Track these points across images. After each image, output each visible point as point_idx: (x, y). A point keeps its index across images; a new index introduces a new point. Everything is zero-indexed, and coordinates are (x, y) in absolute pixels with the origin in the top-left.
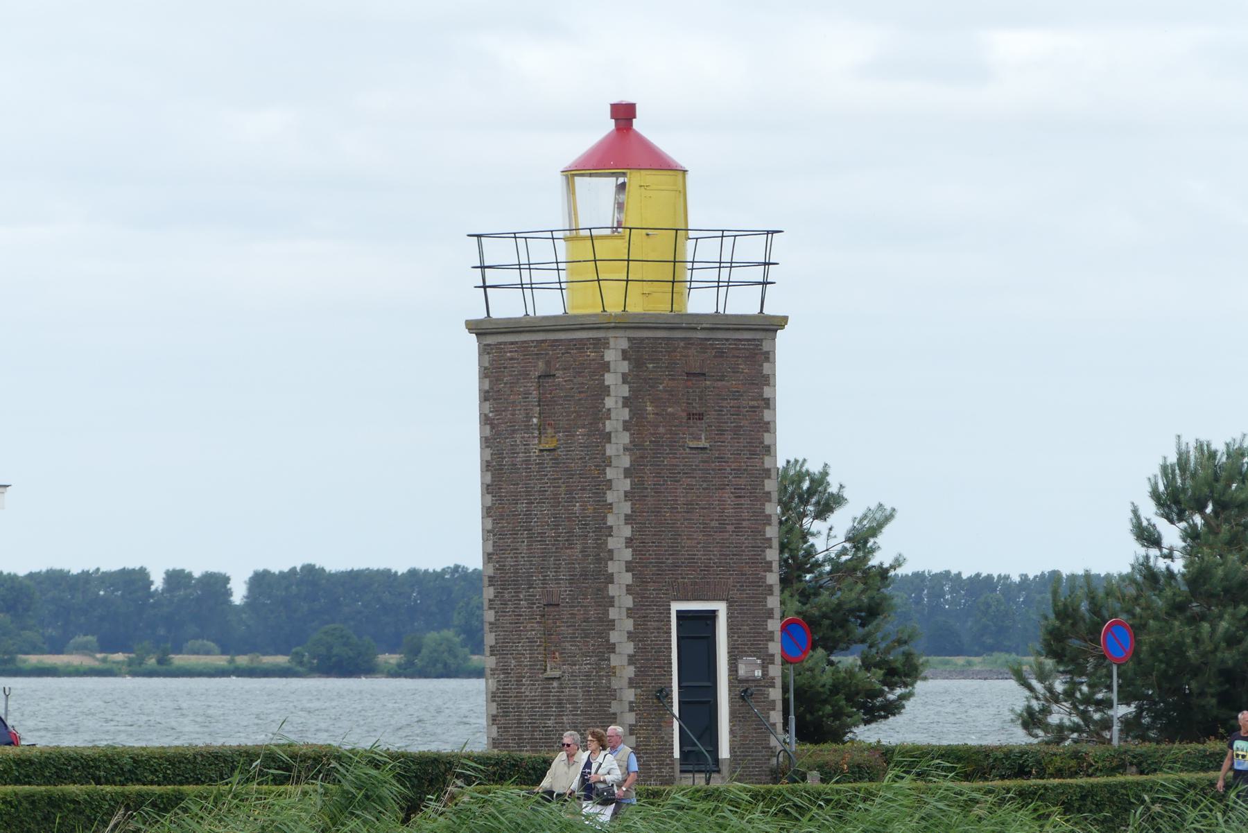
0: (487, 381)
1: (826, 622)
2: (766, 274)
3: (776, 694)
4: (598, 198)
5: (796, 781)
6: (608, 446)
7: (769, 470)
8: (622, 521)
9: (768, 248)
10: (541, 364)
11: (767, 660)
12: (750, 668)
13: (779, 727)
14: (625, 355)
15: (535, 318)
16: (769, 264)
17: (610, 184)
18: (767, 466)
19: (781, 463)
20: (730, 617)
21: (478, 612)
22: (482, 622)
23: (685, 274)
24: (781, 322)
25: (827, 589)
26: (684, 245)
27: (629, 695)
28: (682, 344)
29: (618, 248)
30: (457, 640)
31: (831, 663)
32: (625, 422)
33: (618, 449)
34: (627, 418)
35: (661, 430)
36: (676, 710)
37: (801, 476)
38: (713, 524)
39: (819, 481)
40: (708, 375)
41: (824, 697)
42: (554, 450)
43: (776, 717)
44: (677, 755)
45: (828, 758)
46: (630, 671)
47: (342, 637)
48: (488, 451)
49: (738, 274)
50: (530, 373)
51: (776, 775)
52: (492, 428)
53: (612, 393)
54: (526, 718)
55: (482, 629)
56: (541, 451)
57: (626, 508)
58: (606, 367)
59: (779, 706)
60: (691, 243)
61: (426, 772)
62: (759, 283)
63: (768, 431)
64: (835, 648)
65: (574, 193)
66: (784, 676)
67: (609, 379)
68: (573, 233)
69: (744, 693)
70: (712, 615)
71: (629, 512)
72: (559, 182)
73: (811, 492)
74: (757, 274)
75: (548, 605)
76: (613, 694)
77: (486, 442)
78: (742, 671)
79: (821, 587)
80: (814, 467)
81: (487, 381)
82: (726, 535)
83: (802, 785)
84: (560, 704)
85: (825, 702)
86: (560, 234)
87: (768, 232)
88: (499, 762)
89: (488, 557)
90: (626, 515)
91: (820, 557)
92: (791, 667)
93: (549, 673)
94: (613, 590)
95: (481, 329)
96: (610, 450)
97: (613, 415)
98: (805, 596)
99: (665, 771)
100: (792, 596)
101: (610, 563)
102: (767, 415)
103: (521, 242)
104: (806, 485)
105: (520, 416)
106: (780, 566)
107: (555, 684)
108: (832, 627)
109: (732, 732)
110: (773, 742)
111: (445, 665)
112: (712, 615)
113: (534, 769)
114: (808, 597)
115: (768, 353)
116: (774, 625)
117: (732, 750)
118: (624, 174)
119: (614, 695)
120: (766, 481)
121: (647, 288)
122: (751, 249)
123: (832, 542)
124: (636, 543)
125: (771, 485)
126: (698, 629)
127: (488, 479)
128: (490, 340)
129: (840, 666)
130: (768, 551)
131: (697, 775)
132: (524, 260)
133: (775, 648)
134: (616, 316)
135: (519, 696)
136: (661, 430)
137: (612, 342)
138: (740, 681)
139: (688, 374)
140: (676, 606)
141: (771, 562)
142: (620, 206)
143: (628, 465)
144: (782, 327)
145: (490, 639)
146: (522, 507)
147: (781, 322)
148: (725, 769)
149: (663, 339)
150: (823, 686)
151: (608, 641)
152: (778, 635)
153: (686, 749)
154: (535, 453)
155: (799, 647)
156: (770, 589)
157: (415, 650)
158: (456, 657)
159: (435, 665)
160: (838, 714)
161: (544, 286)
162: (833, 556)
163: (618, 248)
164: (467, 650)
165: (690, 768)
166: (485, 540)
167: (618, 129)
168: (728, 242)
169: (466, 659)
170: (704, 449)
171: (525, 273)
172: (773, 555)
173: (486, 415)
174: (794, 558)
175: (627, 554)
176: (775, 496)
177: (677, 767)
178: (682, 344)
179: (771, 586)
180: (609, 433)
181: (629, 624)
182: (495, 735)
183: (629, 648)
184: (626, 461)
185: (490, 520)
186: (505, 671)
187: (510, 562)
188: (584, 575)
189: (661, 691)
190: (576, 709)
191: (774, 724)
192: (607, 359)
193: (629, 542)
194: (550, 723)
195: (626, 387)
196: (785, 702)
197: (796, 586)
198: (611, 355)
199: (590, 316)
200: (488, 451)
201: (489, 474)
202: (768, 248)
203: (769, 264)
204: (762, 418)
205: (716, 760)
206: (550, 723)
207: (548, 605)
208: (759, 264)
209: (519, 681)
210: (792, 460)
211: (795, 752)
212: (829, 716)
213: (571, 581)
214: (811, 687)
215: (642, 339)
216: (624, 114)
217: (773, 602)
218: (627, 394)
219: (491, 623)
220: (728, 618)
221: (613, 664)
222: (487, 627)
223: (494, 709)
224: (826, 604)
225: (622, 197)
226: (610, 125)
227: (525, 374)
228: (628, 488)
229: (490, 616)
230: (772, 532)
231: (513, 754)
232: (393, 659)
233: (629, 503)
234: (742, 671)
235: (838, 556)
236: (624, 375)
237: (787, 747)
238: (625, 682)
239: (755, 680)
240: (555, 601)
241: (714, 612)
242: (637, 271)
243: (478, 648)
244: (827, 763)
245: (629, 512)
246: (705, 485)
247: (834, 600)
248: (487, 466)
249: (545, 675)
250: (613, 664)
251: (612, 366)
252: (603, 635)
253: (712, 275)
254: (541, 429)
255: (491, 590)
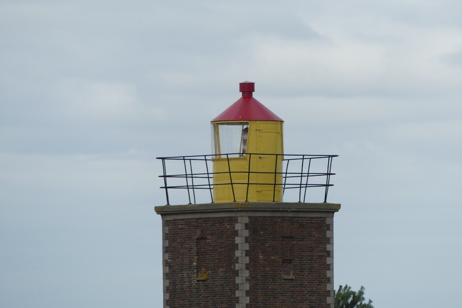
0: (167, 241)
2: (328, 180)
6: (237, 278)
7: (329, 291)
9: (329, 166)
10: (198, 232)
15: (195, 205)
16: (330, 174)
17: (237, 130)
19: (336, 288)
24: (336, 208)
26: (281, 164)
28: (280, 220)
29: (244, 165)
32: (246, 264)
33: (242, 279)
34: (248, 262)
35: (268, 269)
48: (168, 281)
49: (312, 180)
52: (170, 268)
53: (239, 248)
56: (198, 281)
58: (236, 233)
62: (324, 185)
63: (329, 269)
67: (238, 240)
72: (209, 128)
74: (323, 180)
77: (166, 276)
80: (355, 289)
81: (167, 241)
86: (210, 158)
87: (329, 156)
95: (163, 211)
96: (238, 280)
97: (240, 261)
103: (187, 162)
104: (350, 301)
115: (329, 225)
118: (247, 124)
120: (328, 298)
121: (260, 188)
122: (320, 166)
127: (168, 298)
128: (169, 218)
132: (189, 172)
134: (242, 204)
136: (268, 269)
137: (239, 219)
139: (283, 237)
142: (244, 142)
144: (337, 210)
147: (336, 208)
149: (269, 217)
154: (194, 282)
161: (201, 187)
163: (244, 165)
167: (244, 97)
168: (306, 162)
171: (190, 180)
173: (166, 261)
178: (280, 220)
180: (238, 271)
184: (247, 287)
192: (236, 229)
195: (247, 245)
198: (238, 227)
200: (168, 281)
201: (168, 294)
202: (329, 166)
203: (330, 174)
208: (324, 174)
215: (257, 217)
216: (247, 89)
225: (246, 137)
226: (239, 95)
228: (248, 302)
242: (254, 178)
246: (292, 300)
248: (167, 290)
251: (239, 232)
253: (298, 181)
254: (198, 268)
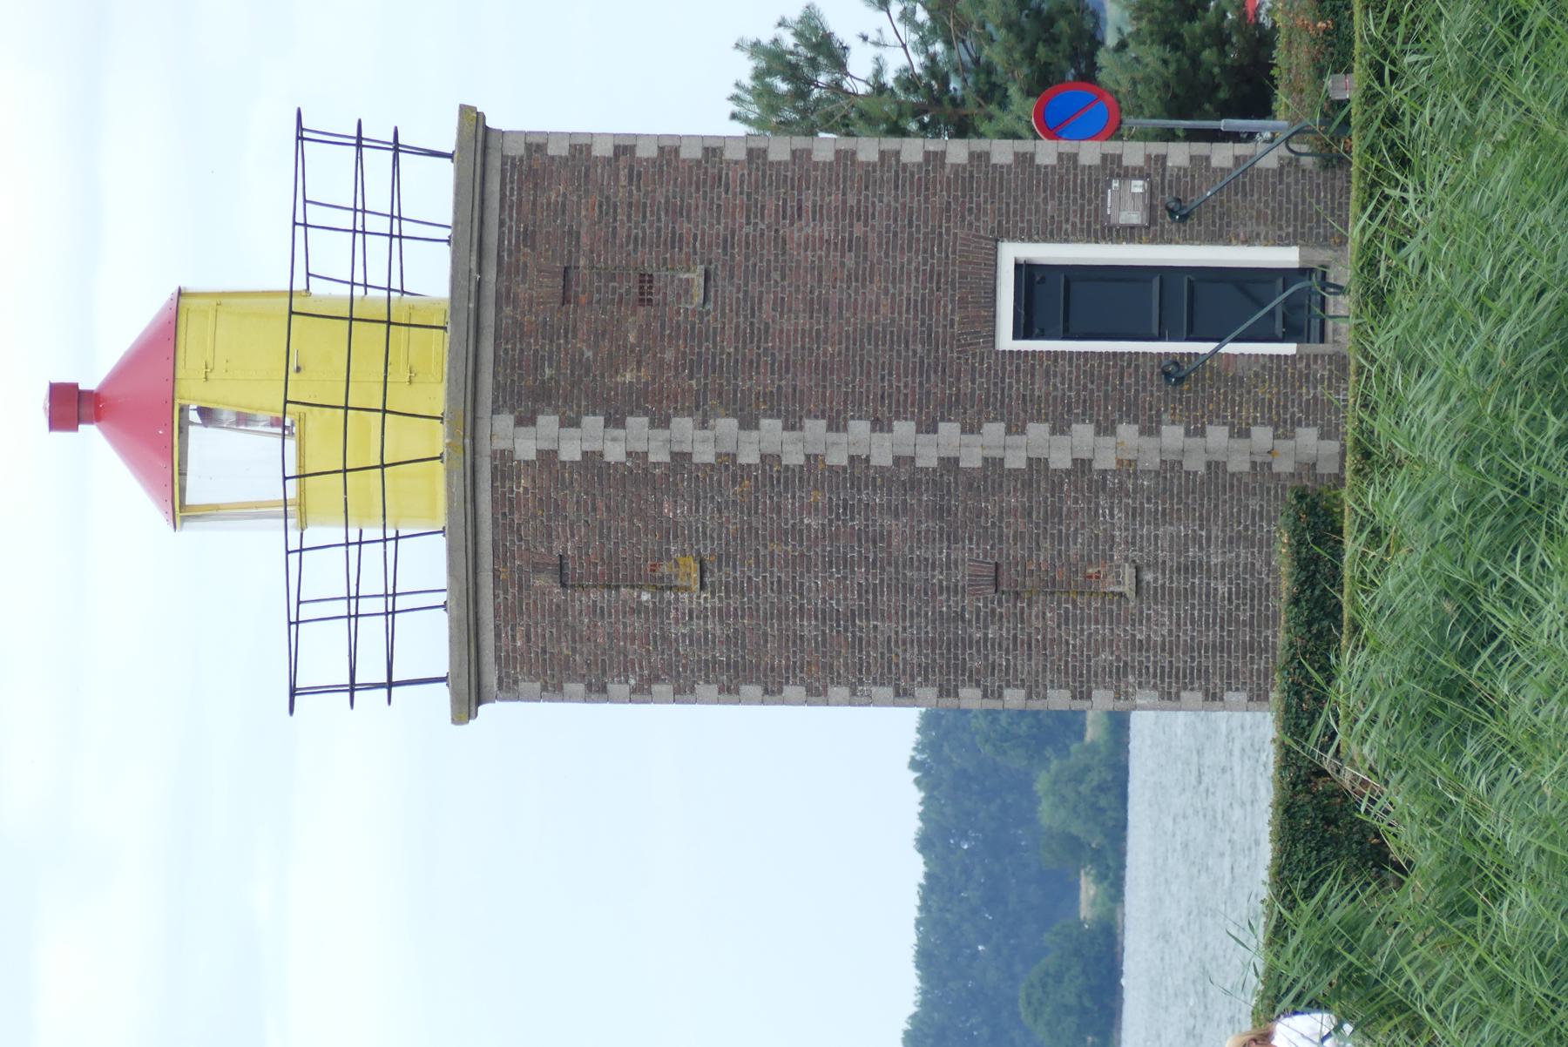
0: (568, 687)
1: (1042, 52)
2: (378, 146)
3: (1179, 154)
4: (226, 461)
5: (1346, 122)
6: (696, 459)
7: (750, 152)
8: (841, 437)
9: (331, 139)
10: (538, 582)
11: (1113, 168)
12: (1128, 202)
13: (1241, 149)
14: (526, 420)
15: (451, 589)
16: (359, 137)
17: (203, 443)
18: (742, 156)
19: (740, 129)
20: (1029, 236)
21: (1003, 720)
22: (1022, 713)
23: (374, 300)
24: (472, 121)
25: (980, 48)
26: (321, 300)
27: (1173, 435)
28: (508, 310)
29: (322, 428)
30: (1054, 765)
31: (1122, 46)
32: (652, 425)
33: (701, 440)
34: (645, 420)
35: (669, 355)
36: (1205, 348)
37: (764, 94)
38: (850, 260)
39: (772, 60)
40: (565, 258)
41: (1186, 62)
42: (702, 562)
43: (1222, 155)
44: (1289, 349)
45: (1304, 58)
46: (1128, 432)
47: (1044, 985)
48: (701, 688)
49: (378, 198)
50: (561, 600)
51: (1333, 161)
52: (657, 679)
53: (597, 447)
54: (1211, 636)
55: (1038, 712)
56: (703, 586)
57: (815, 428)
58: (548, 457)
59: (1201, 148)
60: (317, 287)
61: (1311, 830)
62: (396, 159)
63: (676, 150)
64: (1093, 37)
65: (217, 507)
66: (1145, 136)
67: (570, 451)
68: (293, 512)
69: (1175, 213)
70: (1027, 273)
71: (823, 423)
72: (193, 533)
73: (792, 72)
74: (379, 162)
75: (997, 585)
76: (1171, 467)
77: (683, 693)
78: (1133, 216)
79: (976, 61)
80: (744, 68)
81: (568, 687)
82: (873, 237)
83: (1354, 108)
84: (1187, 569)
85: (1195, 61)
86: (294, 537)
87: (300, 138)
88: (1296, 690)
89: (903, 695)
90: (829, 428)
91: (918, 60)
92: (1129, 121)
93: (1128, 587)
94: (971, 459)
95: (469, 696)
96: (705, 454)
97: (640, 447)
98: (992, 92)
99: (1321, 371)
100: (990, 118)
101: (920, 463)
102: (646, 152)
103: (307, 612)
104: (783, 86)
105: (637, 624)
106: (938, 135)
107: (1148, 576)
108: (1053, 40)
109: (1248, 241)
110: (1270, 162)
111: (1101, 788)
112: (1027, 273)
113: (1309, 624)
114: (994, 86)
115: (528, 146)
116: (1047, 152)
117: (1282, 241)
118: (183, 410)
119: (1173, 463)
120: (772, 157)
121: (398, 374)
122: (330, 171)
123: (890, 37)
124: (883, 411)
125: (780, 149)
126: (1050, 299)
127: (755, 690)
128: (491, 678)
129: (1128, 29)
130: (904, 158)
131: (1331, 311)
132: (341, 608)
133: (1090, 152)
134: (451, 434)
135: (1168, 647)
136: (669, 355)
137: (500, 444)
138: (1152, 220)
139: (565, 300)
140: (1006, 340)
141: (927, 154)
142: (243, 420)
143: (734, 422)
144: (480, 117)
145: (1059, 699)
146: (808, 628)
147: (472, 121)
148: (1320, 256)
149: (497, 346)
150: (1165, 62)
151: (1068, 472)
152: (1066, 146)
153: (1279, 328)
154: (707, 600)
155: (1092, 103)
156: (979, 158)
157: (1073, 847)
158: (1087, 769)
159: (1102, 811)
160: (1219, 38)
161: (391, 569)
162: (915, 37)
163: (322, 428)
164: (1074, 747)
165: (1315, 323)
166: (870, 701)
167: (96, 417)
168: (315, 215)
169: (1092, 749)
170: (707, 276)
171: (365, 606)
172: (913, 150)
173: (633, 691)
174: (917, 112)
175: (904, 429)
176: (800, 142)
177: (1314, 348)
178: (508, 310)
179: (972, 155)
180: (673, 455)
181: (1038, 431)
182: (1242, 697)
183: (1083, 433)
184: (727, 426)
185: (834, 691)
186: (1121, 672)
187: (912, 655)
188: (940, 512)
189: (1167, 375)
190: (1196, 539)
191: (1237, 158)
192: (532, 456)
193: (879, 425)
194: (1222, 589)
195: (588, 421)
196: (1193, 136)
197: (971, 108)
198: (526, 447)
199: (449, 485)
200: (701, 688)
201: (744, 689)
202: (331, 139)
203: (359, 137)
204: (564, 161)
205: (1303, 272)
206: (1222, 589)
207: (997, 585)
208: (359, 158)
209: (1141, 647)
210: (733, 107)
211: (1293, 121)
212: (1223, 53)
213: (952, 538)
214: (1166, 85)
215: (497, 387)
216: (69, 406)
217: (1003, 152)
218: (601, 420)
219: (1029, 696)
220: (1031, 239)
221: (1112, 465)
222: (1036, 705)
223: (1192, 697)
224: (1009, 51)
225: (227, 416)
226: (90, 433)
227: (559, 611)
228: (778, 424)
229: (1014, 698)
230: (868, 149)
231: (1280, 661)
232: (1088, 889)
233: (808, 423)
234: (1133, 216)
235: (917, 27)
236: (563, 424)
237: (1281, 136)
238: (1149, 443)
239: (1151, 191)
240: (988, 571)
241: (1018, 267)
242: (366, 393)
243: (1071, 723)
244: (1315, 60)
245: (823, 423)
246: (776, 276)
247: (1000, 35)
248: (729, 693)
249: (1131, 594)
250: (1112, 465)
251: (545, 446)
252: (1056, 480)
253: (377, 246)
254: (661, 586)
255: (965, 692)
